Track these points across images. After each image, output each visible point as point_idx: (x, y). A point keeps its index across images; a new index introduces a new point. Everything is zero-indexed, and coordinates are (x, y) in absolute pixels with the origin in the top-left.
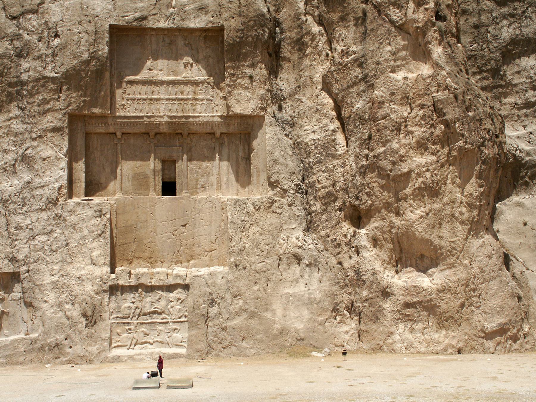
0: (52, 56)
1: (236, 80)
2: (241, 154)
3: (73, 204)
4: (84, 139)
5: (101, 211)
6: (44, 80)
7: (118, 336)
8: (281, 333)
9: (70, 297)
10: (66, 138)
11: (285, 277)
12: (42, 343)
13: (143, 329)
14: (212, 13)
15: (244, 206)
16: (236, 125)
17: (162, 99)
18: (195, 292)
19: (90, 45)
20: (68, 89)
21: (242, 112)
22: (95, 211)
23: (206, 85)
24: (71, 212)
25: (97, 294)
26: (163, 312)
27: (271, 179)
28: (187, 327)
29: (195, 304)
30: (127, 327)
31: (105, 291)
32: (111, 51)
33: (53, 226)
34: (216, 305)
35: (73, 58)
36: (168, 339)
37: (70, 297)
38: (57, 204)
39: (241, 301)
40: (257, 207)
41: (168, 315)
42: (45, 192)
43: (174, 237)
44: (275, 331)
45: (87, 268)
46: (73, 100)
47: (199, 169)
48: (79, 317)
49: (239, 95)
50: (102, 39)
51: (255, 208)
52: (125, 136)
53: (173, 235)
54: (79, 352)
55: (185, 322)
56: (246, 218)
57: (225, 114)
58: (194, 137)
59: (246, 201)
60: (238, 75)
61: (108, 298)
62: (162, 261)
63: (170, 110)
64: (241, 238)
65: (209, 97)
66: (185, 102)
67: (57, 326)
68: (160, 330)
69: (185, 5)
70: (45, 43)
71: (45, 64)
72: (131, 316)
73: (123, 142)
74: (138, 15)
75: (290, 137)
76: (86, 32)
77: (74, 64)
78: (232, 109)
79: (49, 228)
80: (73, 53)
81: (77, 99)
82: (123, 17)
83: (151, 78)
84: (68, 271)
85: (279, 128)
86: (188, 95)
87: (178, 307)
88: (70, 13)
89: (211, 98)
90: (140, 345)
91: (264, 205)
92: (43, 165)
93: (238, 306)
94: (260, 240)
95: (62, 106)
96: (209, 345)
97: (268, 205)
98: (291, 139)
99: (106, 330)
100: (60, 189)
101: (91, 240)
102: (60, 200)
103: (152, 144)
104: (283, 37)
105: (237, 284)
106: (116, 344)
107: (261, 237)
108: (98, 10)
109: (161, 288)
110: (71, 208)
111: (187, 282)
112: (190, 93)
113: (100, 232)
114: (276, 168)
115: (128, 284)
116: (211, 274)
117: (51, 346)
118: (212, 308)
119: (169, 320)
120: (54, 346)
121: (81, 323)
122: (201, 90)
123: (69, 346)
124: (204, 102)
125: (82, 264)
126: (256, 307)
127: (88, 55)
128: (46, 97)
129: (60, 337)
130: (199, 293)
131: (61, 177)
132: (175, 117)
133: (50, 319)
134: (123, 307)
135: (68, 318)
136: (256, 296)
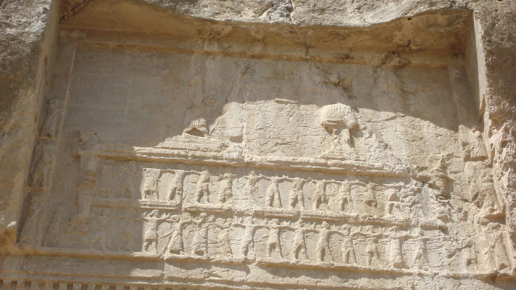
17: (241, 214)
23: (413, 185)
65: (433, 218)
83: (198, 153)
89: (440, 223)
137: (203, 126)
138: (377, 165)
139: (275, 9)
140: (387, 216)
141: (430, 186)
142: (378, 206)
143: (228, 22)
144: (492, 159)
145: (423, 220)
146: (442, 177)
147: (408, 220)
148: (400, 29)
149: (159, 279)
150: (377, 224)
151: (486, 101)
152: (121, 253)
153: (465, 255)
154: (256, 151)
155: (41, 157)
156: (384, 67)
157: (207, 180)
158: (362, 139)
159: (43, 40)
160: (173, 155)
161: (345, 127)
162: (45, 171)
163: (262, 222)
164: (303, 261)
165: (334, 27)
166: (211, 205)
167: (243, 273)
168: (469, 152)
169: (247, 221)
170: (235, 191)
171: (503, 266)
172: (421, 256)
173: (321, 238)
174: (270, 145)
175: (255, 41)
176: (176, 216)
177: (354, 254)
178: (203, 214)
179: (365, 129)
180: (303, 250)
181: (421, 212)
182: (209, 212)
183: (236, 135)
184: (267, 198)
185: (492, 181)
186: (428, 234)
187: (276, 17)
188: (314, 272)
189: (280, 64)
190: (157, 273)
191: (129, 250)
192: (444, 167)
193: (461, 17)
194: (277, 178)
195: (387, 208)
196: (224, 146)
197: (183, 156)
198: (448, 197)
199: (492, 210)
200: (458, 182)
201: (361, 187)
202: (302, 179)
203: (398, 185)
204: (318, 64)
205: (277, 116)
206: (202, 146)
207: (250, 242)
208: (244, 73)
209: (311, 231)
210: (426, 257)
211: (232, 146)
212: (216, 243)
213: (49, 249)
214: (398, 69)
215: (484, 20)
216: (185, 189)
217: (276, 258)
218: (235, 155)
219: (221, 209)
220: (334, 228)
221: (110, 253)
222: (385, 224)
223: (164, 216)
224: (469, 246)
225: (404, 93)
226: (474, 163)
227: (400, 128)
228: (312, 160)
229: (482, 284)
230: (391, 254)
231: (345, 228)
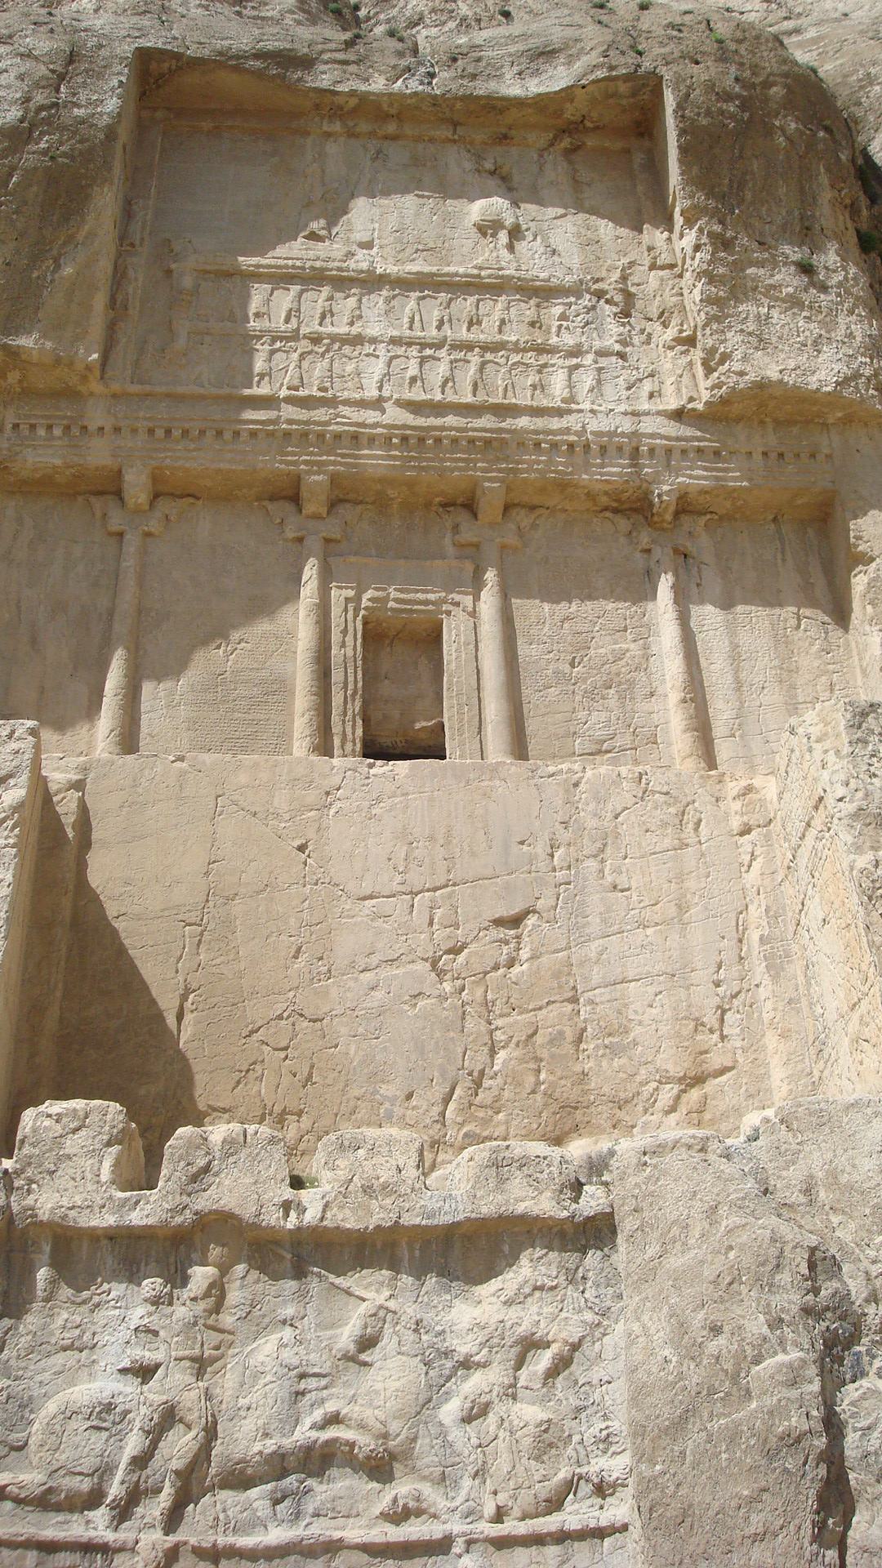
16: (757, 457)
17: (374, 341)
18: (675, 1262)
21: (790, 379)
29: (693, 1352)
52: (165, 506)
53: (441, 974)
55: (600, 1533)
58: (534, 526)
65: (610, 342)
73: (154, 526)
78: (737, 366)
83: (318, 264)
87: (529, 1412)
89: (617, 347)
103: (314, 543)
119: (456, 1527)
124: (588, 359)
130: (719, 1264)
132: (439, 409)
134: (51, 1407)
137: (323, 228)
138: (542, 275)
139: (413, 75)
140: (554, 340)
141: (607, 302)
142: (544, 328)
143: (353, 93)
144: (683, 267)
145: (597, 344)
146: (621, 290)
147: (580, 345)
148: (572, 101)
149: (275, 422)
150: (541, 350)
151: (677, 193)
152: (226, 391)
153: (647, 386)
154: (391, 260)
155: (124, 275)
156: (551, 149)
157: (331, 298)
158: (524, 243)
159: (119, 122)
160: (286, 267)
161: (503, 227)
162: (131, 290)
163: (400, 351)
164: (451, 397)
165: (489, 97)
166: (335, 330)
167: (378, 413)
168: (655, 258)
169: (381, 349)
170: (365, 311)
172: (594, 388)
173: (472, 369)
174: (409, 251)
175: (387, 117)
176: (293, 344)
177: (513, 388)
178: (325, 341)
179: (527, 230)
180: (450, 384)
181: (595, 335)
182: (334, 338)
184: (406, 320)
185: (682, 295)
186: (604, 362)
187: (414, 85)
188: (464, 411)
189: (420, 147)
190: (272, 414)
191: (236, 387)
192: (624, 278)
193: (648, 85)
194: (418, 294)
195: (554, 329)
196: (350, 254)
197: (299, 268)
198: (628, 315)
199: (681, 331)
200: (640, 296)
201: (522, 304)
202: (449, 295)
203: (568, 300)
204: (468, 146)
205: (417, 214)
206: (323, 255)
207: (385, 375)
208: (374, 160)
209: (460, 360)
210: (600, 390)
211: (361, 254)
212: (344, 376)
213: (140, 386)
214: (569, 152)
215: (676, 89)
216: (302, 311)
217: (417, 394)
218: (364, 266)
219: (349, 334)
220: (489, 356)
221: (214, 391)
222: (552, 350)
223: (278, 344)
224: (652, 375)
225: (577, 184)
226: (661, 273)
227: (571, 229)
228: (461, 270)
229: (666, 421)
230: (558, 386)
231: (502, 357)
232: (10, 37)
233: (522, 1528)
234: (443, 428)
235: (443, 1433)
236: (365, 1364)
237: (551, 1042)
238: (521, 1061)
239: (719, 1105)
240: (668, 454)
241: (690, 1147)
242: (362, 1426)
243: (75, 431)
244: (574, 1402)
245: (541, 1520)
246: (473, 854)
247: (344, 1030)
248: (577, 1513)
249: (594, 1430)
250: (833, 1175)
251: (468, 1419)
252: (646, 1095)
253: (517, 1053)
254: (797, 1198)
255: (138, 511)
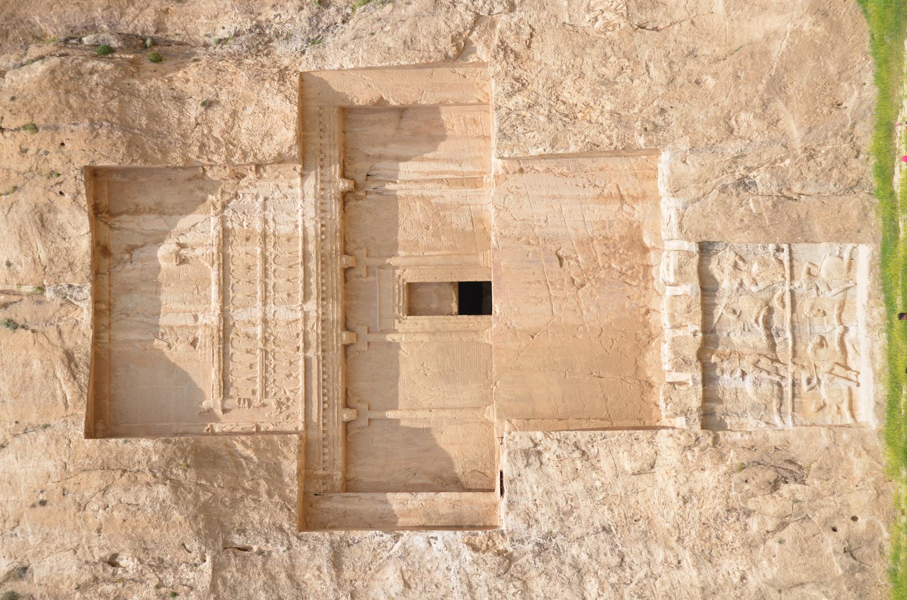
0: (161, 572)
1: (217, 141)
2: (390, 130)
3: (511, 516)
4: (360, 494)
5: (526, 453)
6: (220, 588)
7: (826, 410)
8: (825, 14)
9: (732, 520)
10: (357, 534)
11: (685, 14)
12: (845, 588)
13: (808, 348)
14: (52, 195)
15: (514, 116)
17: (265, 314)
19: (136, 481)
20: (242, 531)
22: (528, 465)
23: (228, 213)
24: (529, 520)
25: (722, 458)
26: (767, 304)
27: (451, 54)
28: (804, 245)
29: (748, 227)
30: (805, 387)
31: (716, 440)
32: (149, 433)
33: (563, 563)
34: (751, 175)
35: (166, 520)
36: (834, 291)
37: (732, 520)
38: (511, 554)
39: (743, 116)
40: (518, 85)
41: (773, 291)
42: (483, 584)
43: (588, 285)
44: (818, 29)
45: (661, 484)
46: (267, 520)
47: (428, 228)
48: (779, 499)
49: (251, 132)
50: (121, 453)
51: (519, 91)
52: (353, 401)
53: (582, 286)
54: (867, 499)
55: (791, 252)
56: (544, 111)
57: (299, 167)
58: (354, 241)
59: (503, 111)
60: (203, 134)
61: (732, 434)
62: (643, 310)
63: (289, 295)
64: (590, 122)
65: (258, 204)
66: (270, 260)
67: (803, 551)
68: (812, 309)
69: (34, 260)
70: (130, 589)
71: (180, 587)
72: (777, 379)
73: (365, 406)
74: (61, 372)
75: (349, 11)
76: (105, 491)
77: (181, 518)
78: (285, 150)
79: (568, 572)
80: (154, 521)
81: (266, 511)
82: (67, 407)
83: (216, 340)
84: (668, 526)
85: (329, 39)
86: (254, 256)
87: (755, 268)
88: (56, 532)
89: (261, 200)
90: (850, 356)
91: (511, 68)
92: (420, 588)
93: (755, 124)
94: (595, 76)
95: (282, 545)
96: (850, 189)
97: (512, 60)
98: (353, 10)
99: (811, 436)
100: (475, 549)
101: (594, 475)
102: (501, 548)
103: (372, 338)
104: (105, 27)
105: (699, 128)
106: (847, 414)
107: (589, 74)
108: (49, 465)
109: (707, 310)
110: (520, 521)
111: (694, 248)
112: (249, 249)
113: (577, 454)
114: (423, 41)
115: (700, 387)
116: (676, 191)
117: (852, 568)
118: (760, 186)
119: (787, 288)
120: (851, 559)
121: (793, 494)
122: (241, 225)
123: (852, 522)
125: (652, 495)
126: (759, 79)
127: (160, 486)
128: (260, 583)
129: (830, 544)
131: (447, 546)
133: (785, 567)
134: (755, 398)
135: (783, 525)
136: (731, 80)
150: (265, 236)
171: (295, 169)
178: (267, 335)
182: (264, 331)
183: (192, 318)
228: (216, 273)
232: (80, 505)
233: (788, 272)
234: (317, 283)
235: (760, 291)
236: (741, 312)
237: (608, 248)
238: (615, 259)
239: (631, 192)
240: (324, 182)
241: (682, 219)
242: (759, 313)
243: (326, 443)
244: (752, 255)
245: (786, 266)
246: (534, 274)
247: (605, 321)
248: (785, 256)
249: (761, 250)
250: (694, 181)
251: (757, 284)
252: (628, 216)
253: (613, 260)
254: (701, 193)
255: (358, 414)
